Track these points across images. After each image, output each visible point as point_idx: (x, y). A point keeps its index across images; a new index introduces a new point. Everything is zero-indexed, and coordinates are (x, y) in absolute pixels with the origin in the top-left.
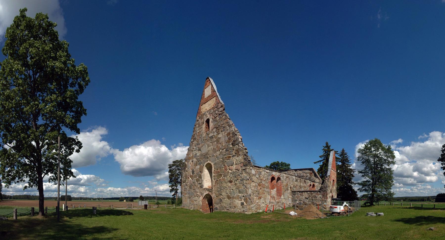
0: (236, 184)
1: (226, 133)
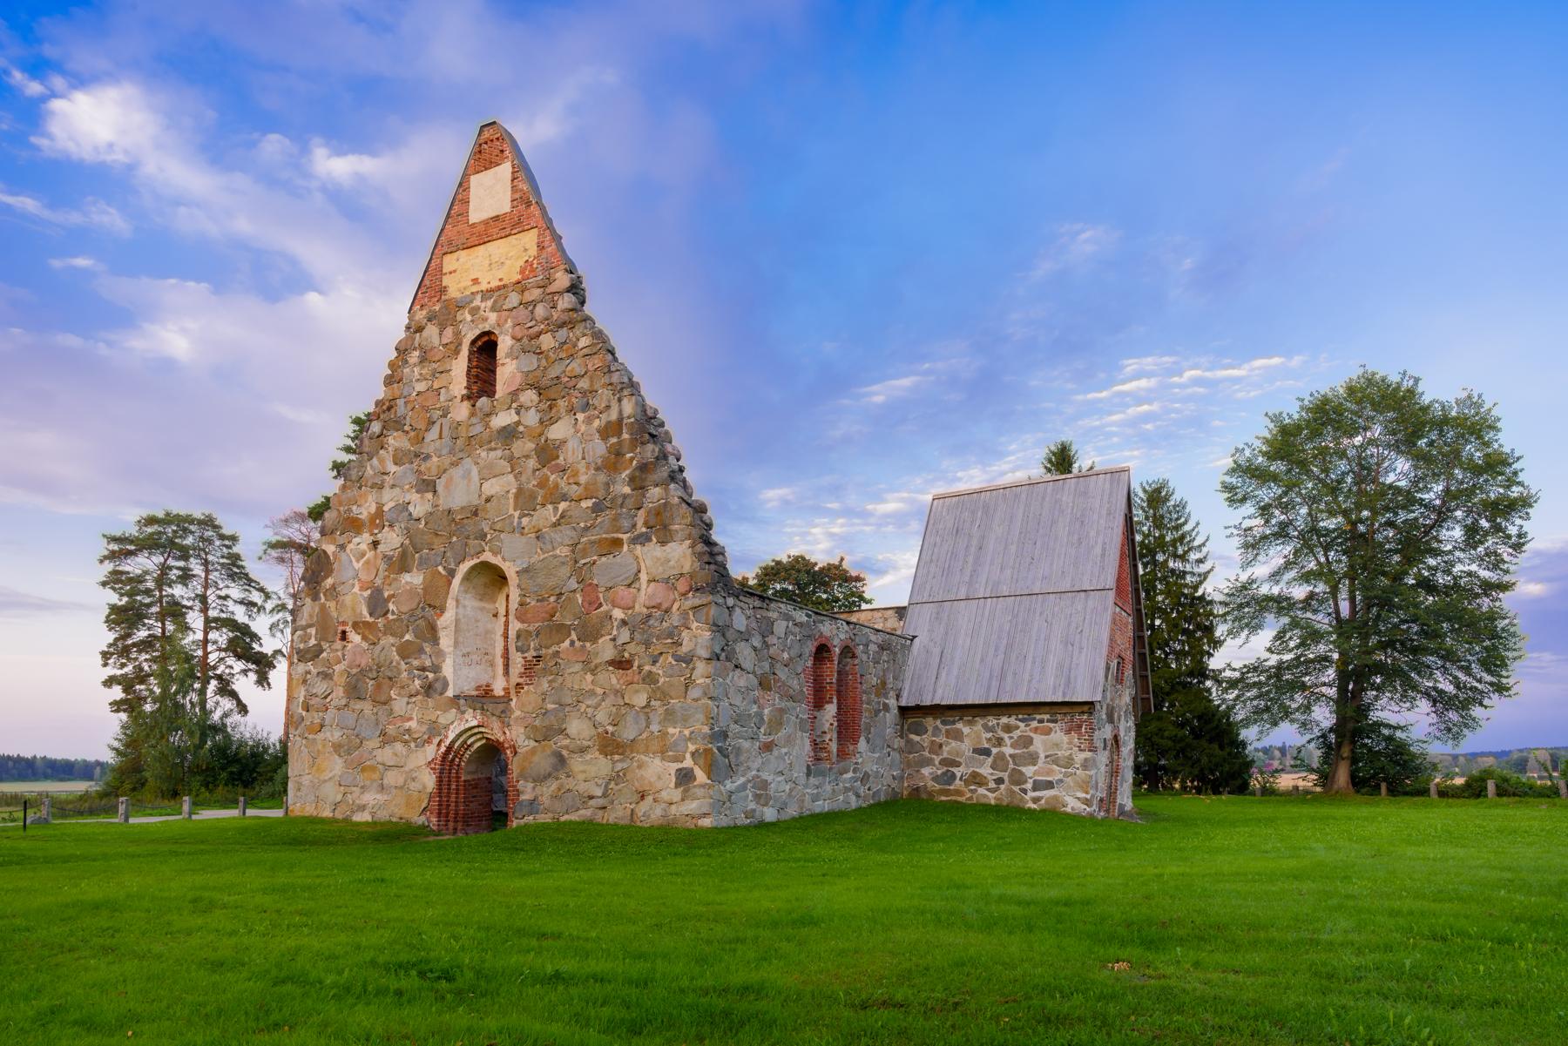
0: (650, 679)
1: (596, 423)
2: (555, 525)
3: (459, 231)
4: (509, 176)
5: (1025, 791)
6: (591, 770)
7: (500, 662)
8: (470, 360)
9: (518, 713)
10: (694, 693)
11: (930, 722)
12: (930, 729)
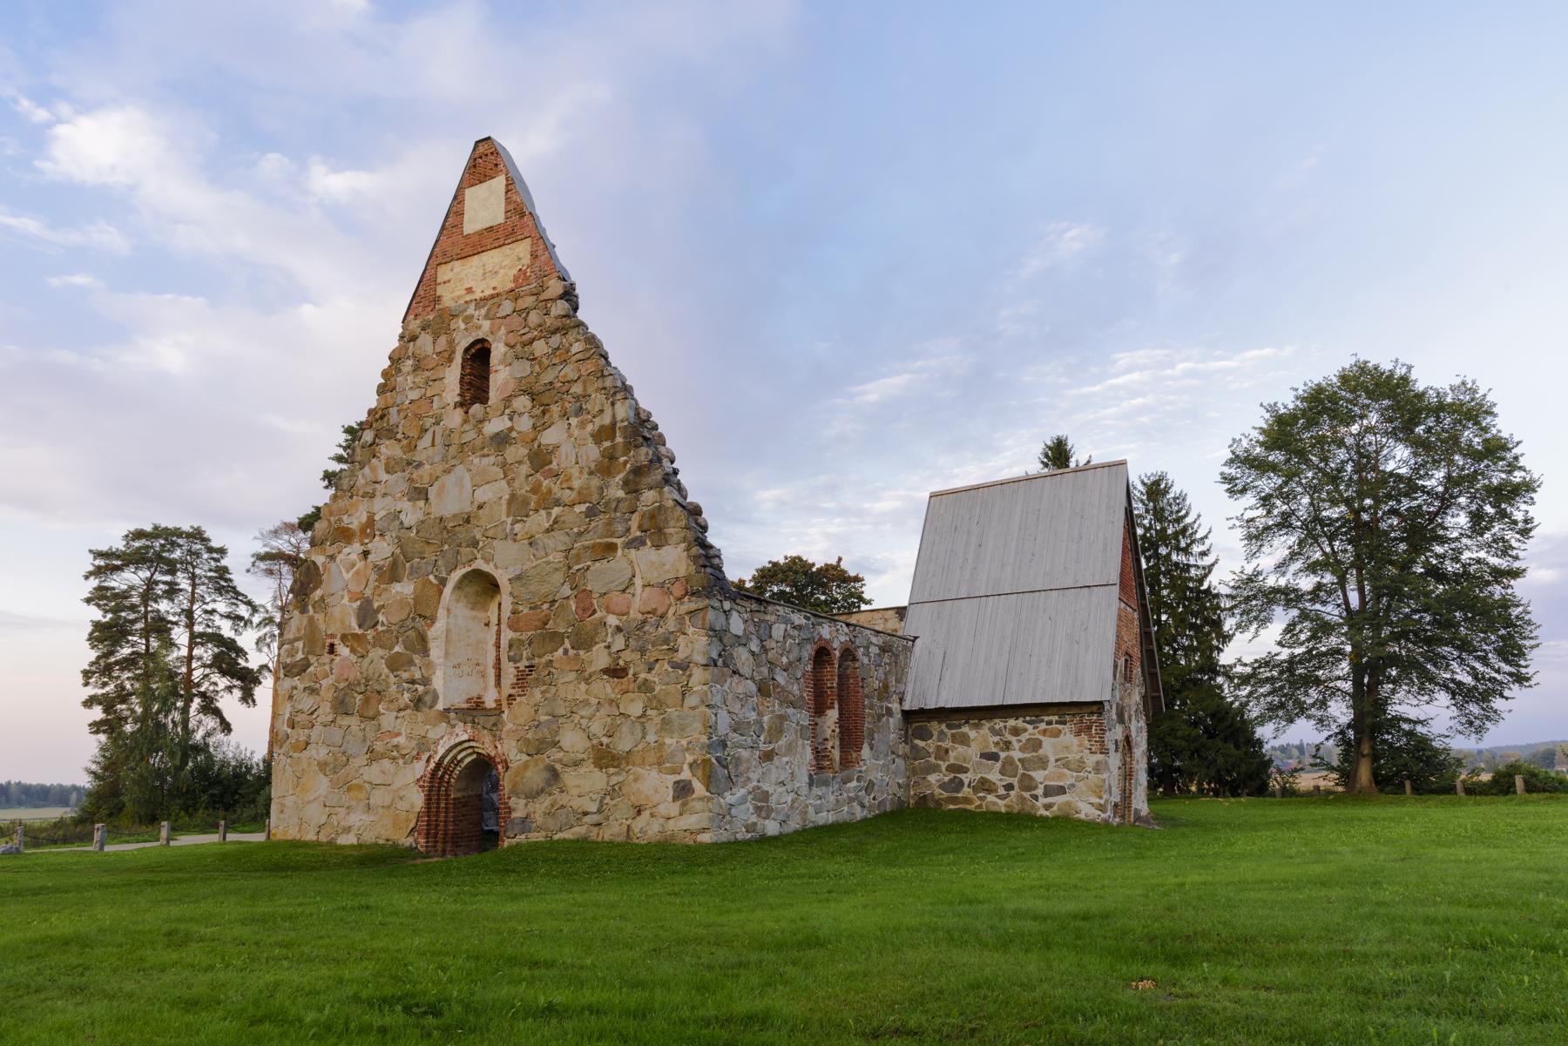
0: (646, 687)
1: (590, 427)
2: (548, 531)
3: (454, 242)
4: (503, 189)
5: (1036, 797)
6: (584, 785)
7: (491, 672)
8: (463, 368)
9: (509, 726)
10: (691, 700)
11: (935, 727)
12: (936, 734)
